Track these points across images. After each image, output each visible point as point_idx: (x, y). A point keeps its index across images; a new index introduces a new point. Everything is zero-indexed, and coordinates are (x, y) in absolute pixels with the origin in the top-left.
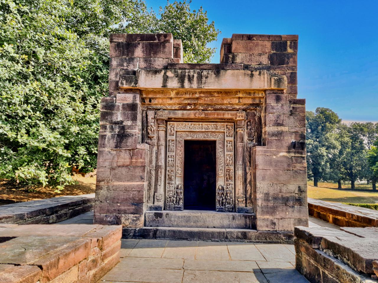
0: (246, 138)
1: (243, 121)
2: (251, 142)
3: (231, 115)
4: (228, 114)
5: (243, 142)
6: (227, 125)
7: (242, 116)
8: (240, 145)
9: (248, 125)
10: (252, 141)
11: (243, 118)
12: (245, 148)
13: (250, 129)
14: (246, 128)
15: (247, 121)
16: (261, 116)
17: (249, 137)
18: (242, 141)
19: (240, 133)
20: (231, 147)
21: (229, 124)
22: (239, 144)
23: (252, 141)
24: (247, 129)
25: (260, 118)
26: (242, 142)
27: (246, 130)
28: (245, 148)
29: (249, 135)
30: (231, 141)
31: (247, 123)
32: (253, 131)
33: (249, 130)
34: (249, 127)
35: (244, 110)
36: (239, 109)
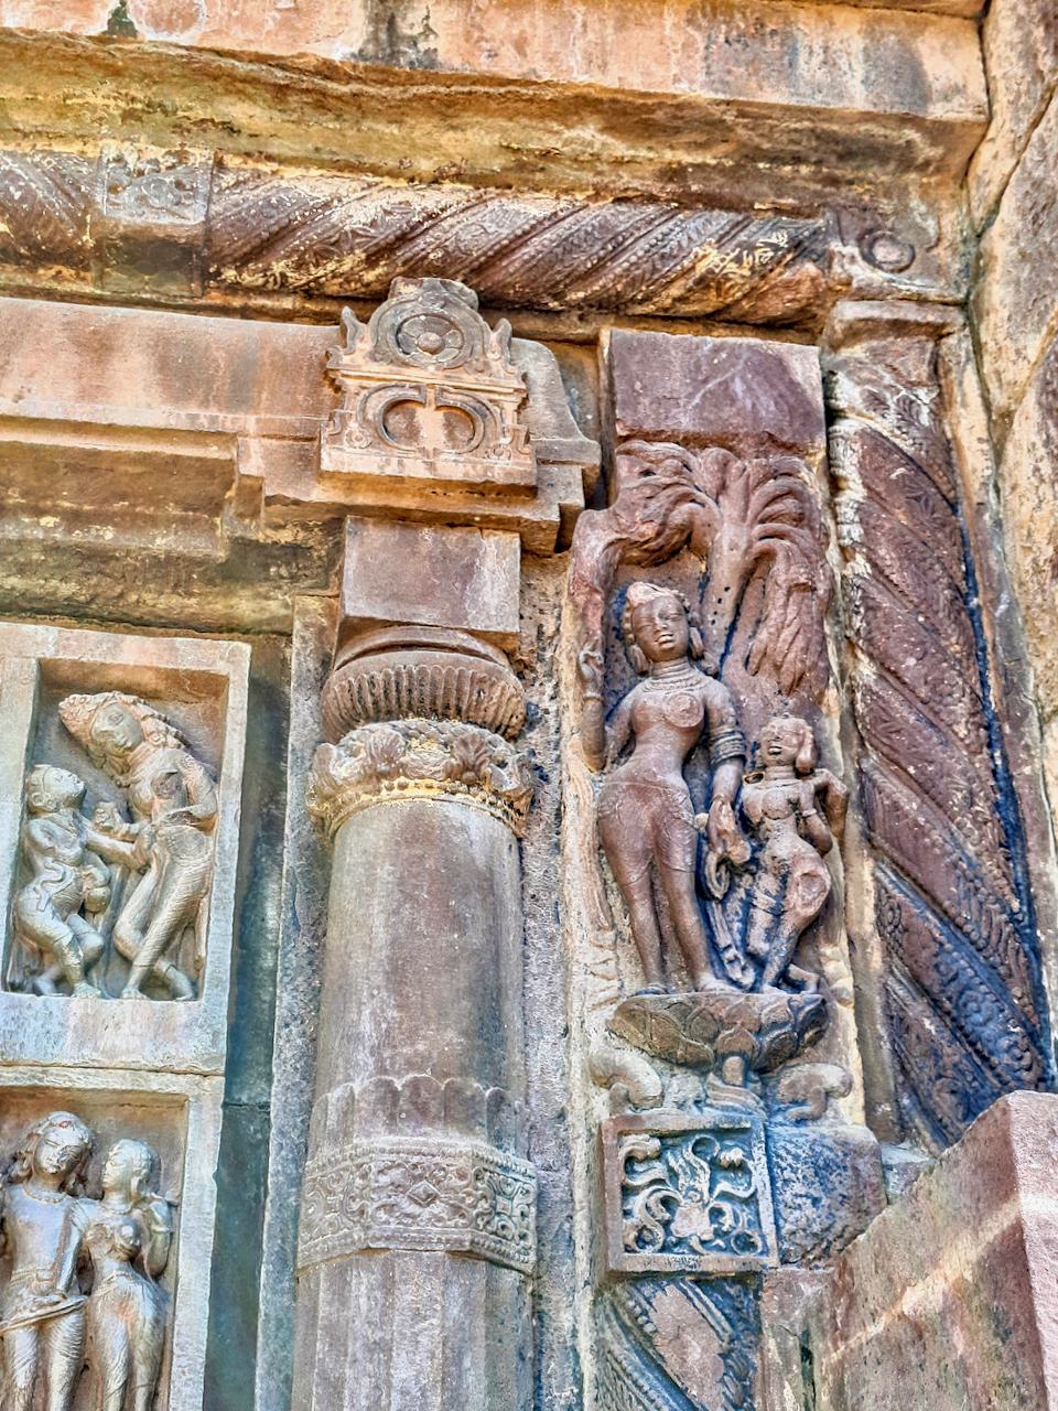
0: (585, 975)
1: (498, 556)
2: (732, 1098)
3: (180, 372)
4: (99, 348)
5: (493, 1115)
6: (53, 684)
7: (466, 418)
8: (418, 1179)
9: (622, 653)
10: (762, 1068)
11: (506, 466)
12: (575, 1315)
13: (699, 745)
14: (567, 710)
15: (593, 541)
16: (947, 449)
17: (670, 952)
18: (478, 1080)
19: (418, 831)
20: (122, 1310)
21: (134, 653)
22: (369, 1161)
23: (762, 1068)
24: (615, 740)
25: (927, 482)
26: (455, 1109)
27: (578, 785)
28: (575, 1315)
29: (682, 899)
30: (152, 1116)
31: (612, 584)
32: (772, 793)
33: (658, 755)
34: (667, 697)
35: (509, 296)
36: (394, 248)
